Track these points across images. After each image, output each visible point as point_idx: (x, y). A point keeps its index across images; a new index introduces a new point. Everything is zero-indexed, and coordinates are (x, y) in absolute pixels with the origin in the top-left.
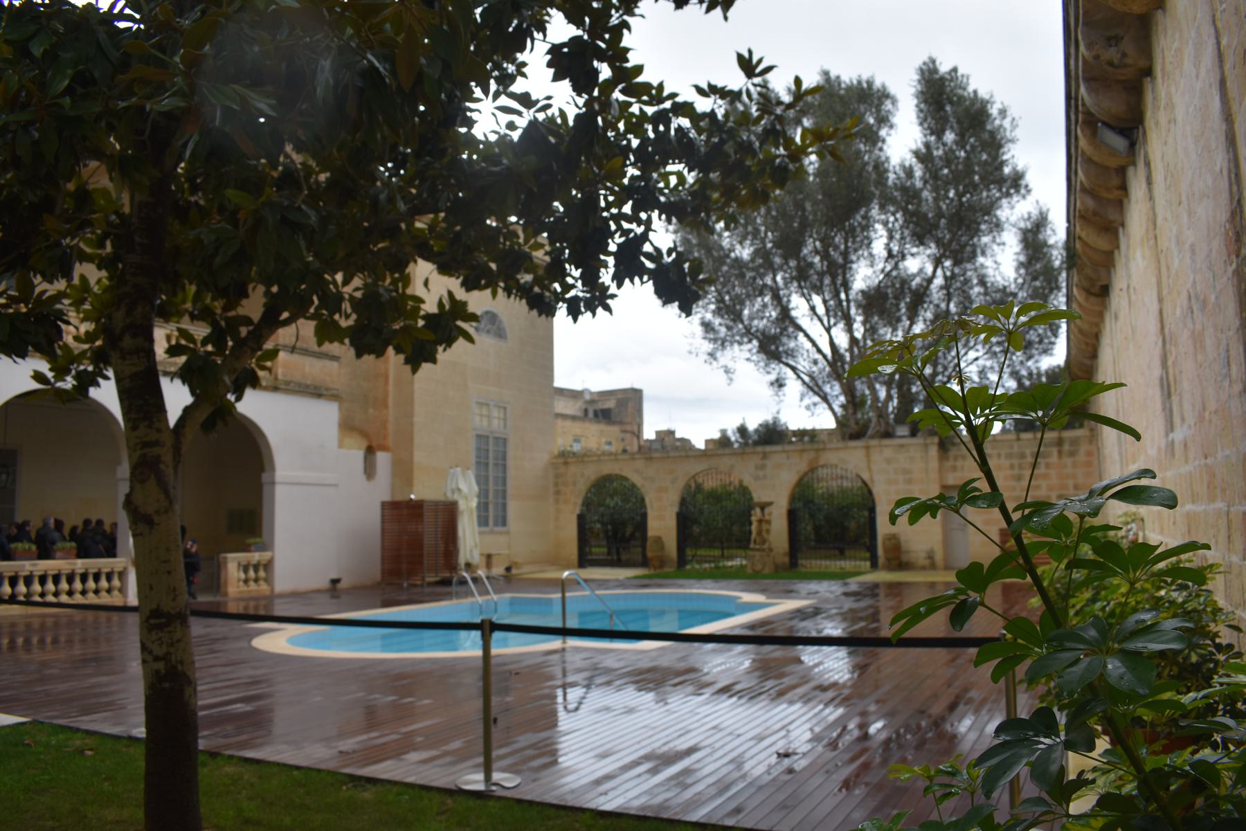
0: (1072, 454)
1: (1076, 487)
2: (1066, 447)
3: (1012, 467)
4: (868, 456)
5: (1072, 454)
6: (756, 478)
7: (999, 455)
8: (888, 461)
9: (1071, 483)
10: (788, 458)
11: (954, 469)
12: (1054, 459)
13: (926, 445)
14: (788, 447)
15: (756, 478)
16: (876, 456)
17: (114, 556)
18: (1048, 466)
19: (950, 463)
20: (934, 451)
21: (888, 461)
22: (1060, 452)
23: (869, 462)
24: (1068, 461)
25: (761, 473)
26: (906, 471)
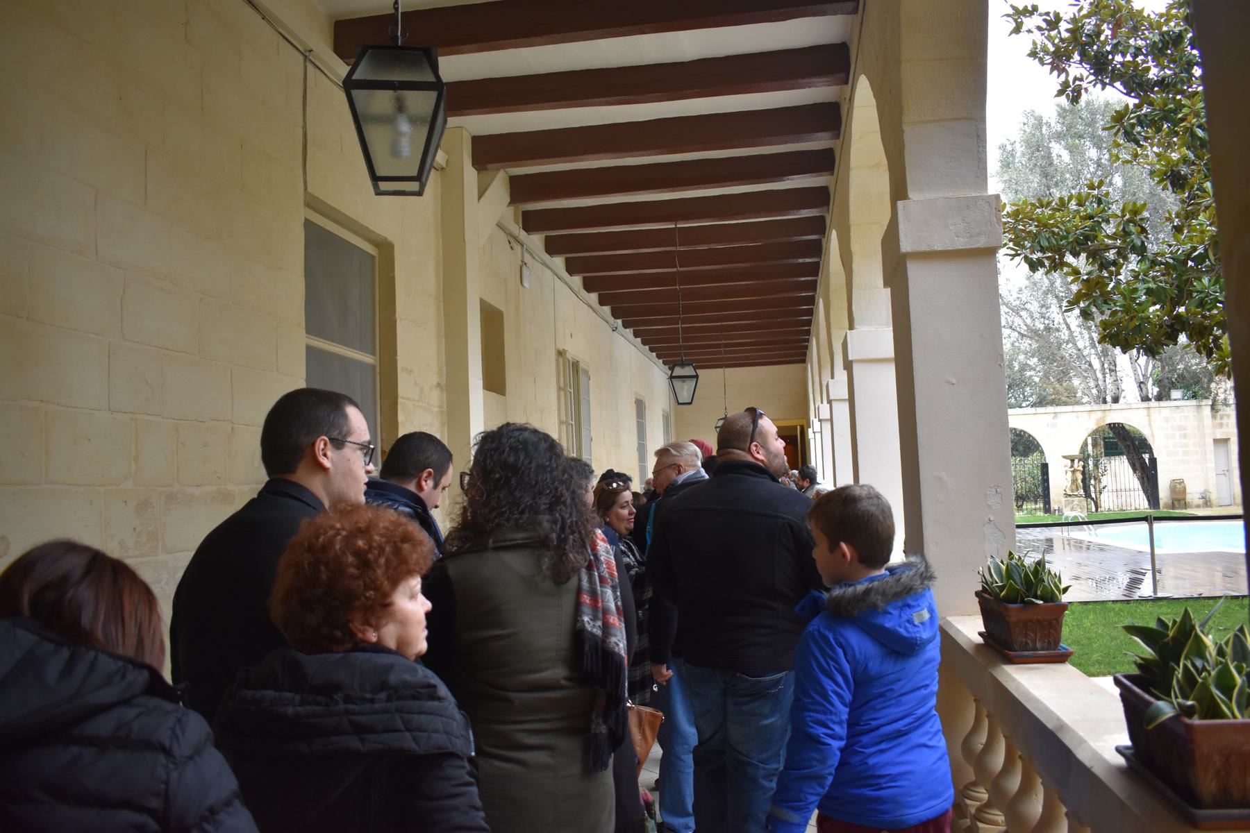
8: (1167, 420)
11: (1221, 425)
13: (1199, 406)
14: (1077, 408)
19: (1218, 421)
20: (1207, 411)
21: (1167, 420)
26: (1181, 428)
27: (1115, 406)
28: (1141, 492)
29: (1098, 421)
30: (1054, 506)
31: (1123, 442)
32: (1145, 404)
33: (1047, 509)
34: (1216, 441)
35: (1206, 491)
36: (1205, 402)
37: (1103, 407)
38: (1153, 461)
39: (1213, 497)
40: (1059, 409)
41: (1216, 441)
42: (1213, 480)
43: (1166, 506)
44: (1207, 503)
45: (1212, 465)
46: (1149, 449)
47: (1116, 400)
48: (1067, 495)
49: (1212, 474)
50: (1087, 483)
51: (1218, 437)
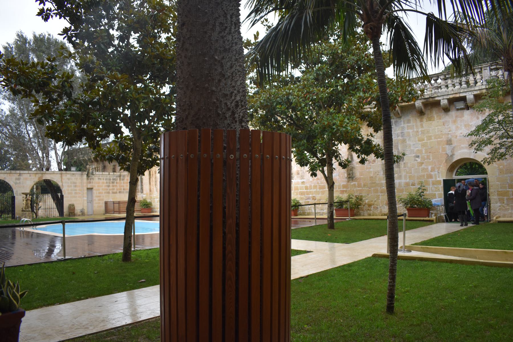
0: (123, 180)
1: (124, 189)
2: (122, 177)
3: (107, 183)
4: (61, 177)
5: (123, 180)
6: (16, 183)
8: (69, 179)
9: (122, 188)
11: (90, 183)
12: (118, 181)
13: (82, 174)
14: (30, 172)
15: (16, 183)
16: (64, 177)
17: (444, 180)
18: (117, 183)
19: (89, 181)
20: (85, 176)
21: (69, 179)
23: (62, 179)
24: (122, 181)
25: (18, 181)
26: (74, 183)
27: (47, 172)
28: (56, 210)
29: (39, 178)
30: (17, 216)
31: (50, 188)
32: (60, 172)
33: (13, 217)
34: (88, 189)
35: (83, 209)
36: (84, 173)
37: (42, 172)
38: (62, 196)
39: (86, 211)
40: (22, 172)
41: (88, 189)
42: (86, 205)
43: (66, 215)
46: (60, 191)
47: (48, 169)
48: (23, 211)
49: (86, 202)
50: (32, 205)
51: (89, 187)
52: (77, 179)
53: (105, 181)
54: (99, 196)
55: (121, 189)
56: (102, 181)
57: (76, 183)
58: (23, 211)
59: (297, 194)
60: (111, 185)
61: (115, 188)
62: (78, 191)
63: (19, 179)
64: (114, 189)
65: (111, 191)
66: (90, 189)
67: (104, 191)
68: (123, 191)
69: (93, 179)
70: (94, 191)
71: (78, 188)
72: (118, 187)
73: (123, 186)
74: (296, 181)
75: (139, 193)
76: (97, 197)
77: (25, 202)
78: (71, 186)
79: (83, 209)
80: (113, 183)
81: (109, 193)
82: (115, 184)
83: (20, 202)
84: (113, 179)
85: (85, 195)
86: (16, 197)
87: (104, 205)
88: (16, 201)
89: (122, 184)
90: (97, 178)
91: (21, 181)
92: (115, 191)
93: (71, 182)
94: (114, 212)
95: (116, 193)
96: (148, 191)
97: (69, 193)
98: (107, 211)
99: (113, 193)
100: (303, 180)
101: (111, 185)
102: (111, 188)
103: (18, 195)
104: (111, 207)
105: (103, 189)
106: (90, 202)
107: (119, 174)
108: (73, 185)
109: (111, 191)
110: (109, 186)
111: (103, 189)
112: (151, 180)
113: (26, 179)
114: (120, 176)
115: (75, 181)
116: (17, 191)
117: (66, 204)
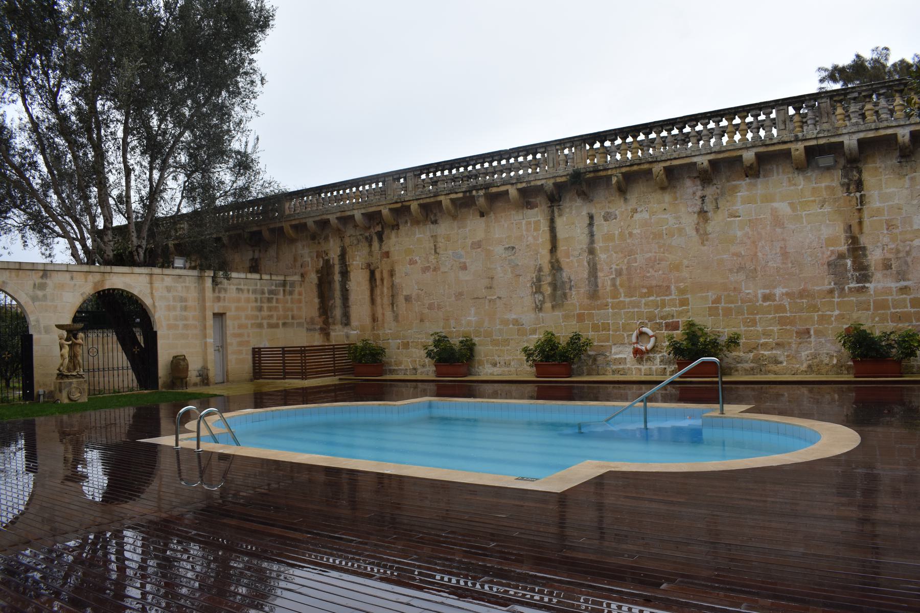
0: (291, 293)
1: (293, 318)
2: (288, 288)
3: (256, 301)
4: (151, 283)
5: (291, 293)
6: (34, 299)
7: (248, 290)
8: (169, 289)
9: (290, 314)
10: (72, 278)
11: (219, 299)
12: (281, 296)
15: (34, 299)
16: (157, 284)
20: (209, 283)
21: (169, 289)
22: (284, 291)
23: (152, 288)
24: (289, 298)
25: (40, 293)
26: (183, 300)
28: (130, 371)
29: (96, 284)
30: (39, 389)
34: (214, 314)
35: (205, 368)
41: (214, 314)
44: (205, 379)
45: (210, 340)
49: (211, 350)
51: (216, 311)
52: (187, 288)
53: (252, 296)
54: (241, 335)
55: (286, 317)
56: (244, 296)
57: (185, 300)
58: (61, 375)
59: (883, 320)
60: (265, 305)
61: (275, 314)
62: (191, 322)
63: (42, 287)
64: (271, 317)
65: (265, 322)
66: (219, 316)
67: (249, 322)
68: (290, 321)
69: (225, 290)
70: (229, 322)
71: (190, 314)
72: (281, 312)
73: (292, 310)
74: (880, 286)
75: (338, 327)
76: (236, 335)
77: (66, 350)
78: (174, 309)
79: (205, 368)
80: (269, 300)
81: (260, 326)
82: (274, 304)
83: (48, 349)
84: (271, 292)
85: (210, 331)
86: (35, 337)
87: (250, 357)
88: (35, 348)
89: (289, 305)
90: (234, 287)
91: (49, 290)
92: (274, 321)
93: (174, 298)
94: (285, 375)
95: (276, 326)
96: (368, 321)
97: (170, 327)
98: (258, 372)
99: (271, 326)
100: (903, 284)
101: (265, 305)
102: (265, 313)
103: (40, 332)
104: (267, 362)
105: (247, 317)
106: (222, 348)
107: (282, 278)
108: (179, 305)
109: (265, 322)
110: (260, 309)
111: (247, 317)
112: (378, 291)
113: (62, 286)
114: (284, 284)
115: (184, 294)
116: (37, 321)
117: (164, 356)
